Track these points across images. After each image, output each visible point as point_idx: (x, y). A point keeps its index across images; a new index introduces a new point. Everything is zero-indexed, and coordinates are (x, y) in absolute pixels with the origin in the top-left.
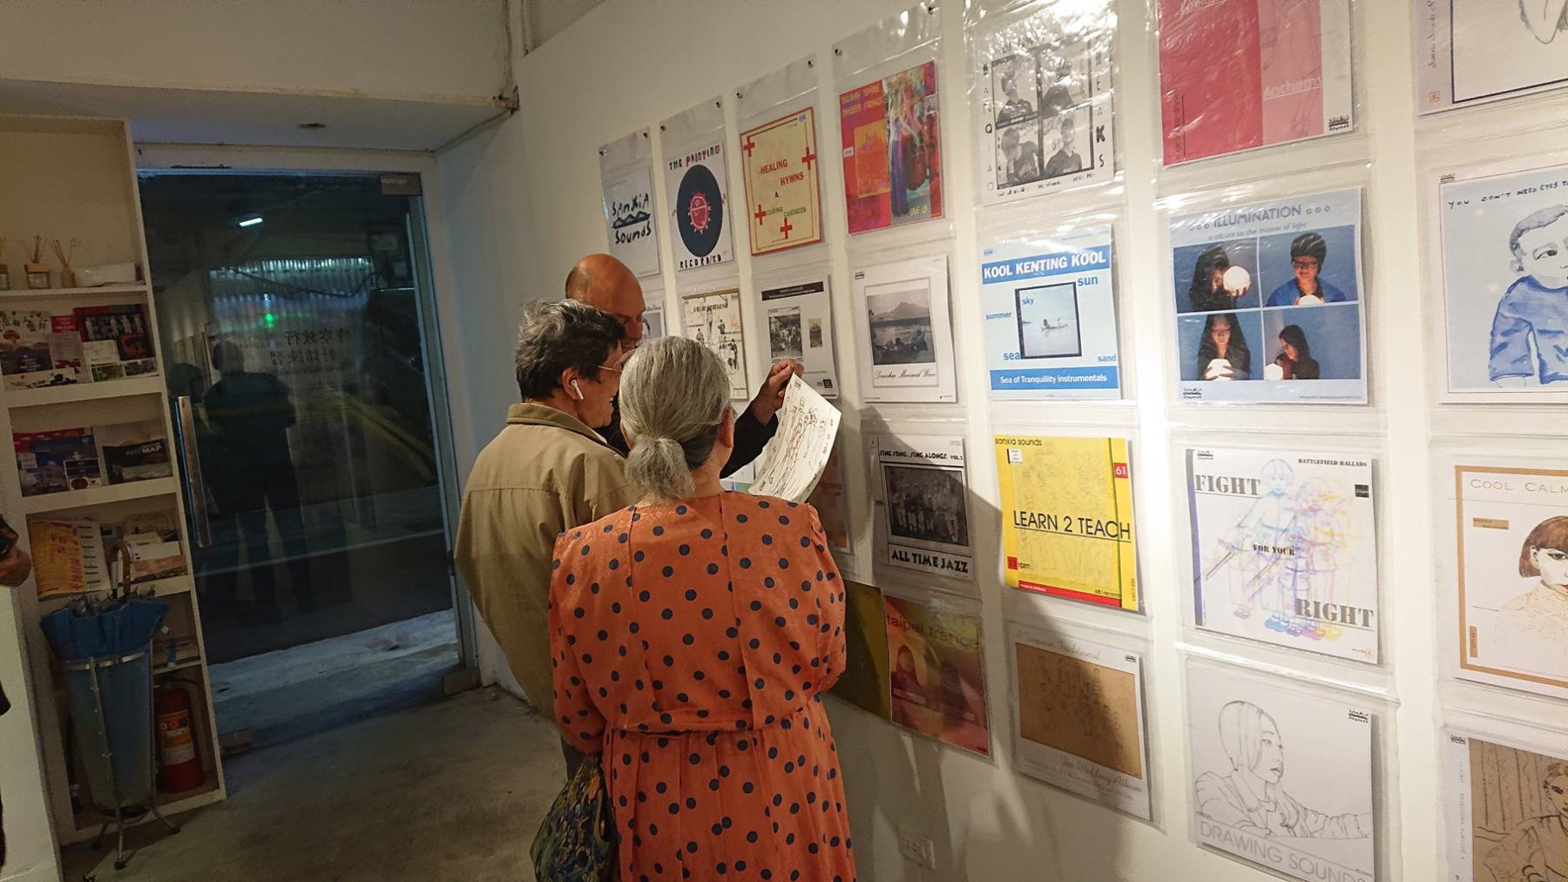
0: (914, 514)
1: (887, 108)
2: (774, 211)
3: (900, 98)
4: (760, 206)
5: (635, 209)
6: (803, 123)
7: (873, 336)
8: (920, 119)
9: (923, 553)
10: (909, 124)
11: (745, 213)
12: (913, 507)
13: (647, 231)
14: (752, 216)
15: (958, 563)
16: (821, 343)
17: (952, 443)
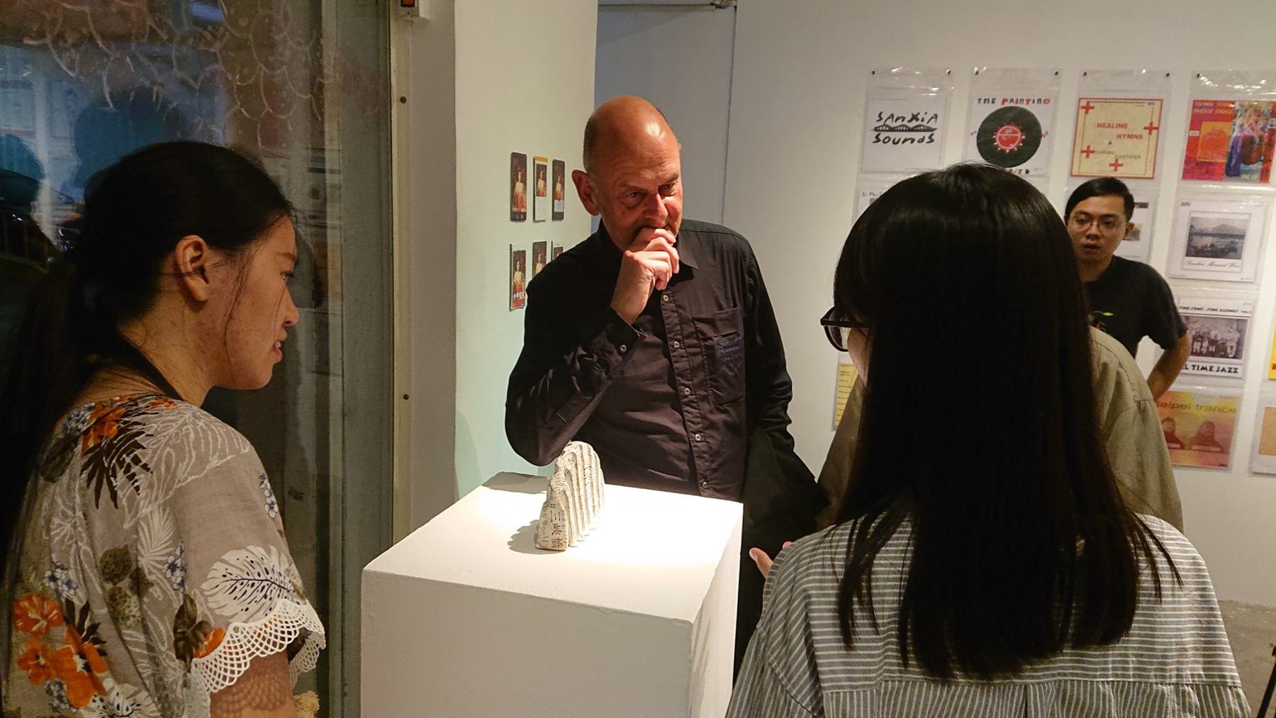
0: (1199, 343)
1: (1235, 116)
2: (1104, 152)
3: (1247, 115)
4: (1089, 147)
5: (914, 121)
6: (1151, 106)
7: (1190, 240)
8: (1262, 129)
9: (1201, 365)
10: (1252, 129)
11: (1070, 145)
12: (1200, 339)
13: (927, 140)
14: (1078, 150)
15: (1231, 368)
16: (1138, 239)
17: (1245, 304)
